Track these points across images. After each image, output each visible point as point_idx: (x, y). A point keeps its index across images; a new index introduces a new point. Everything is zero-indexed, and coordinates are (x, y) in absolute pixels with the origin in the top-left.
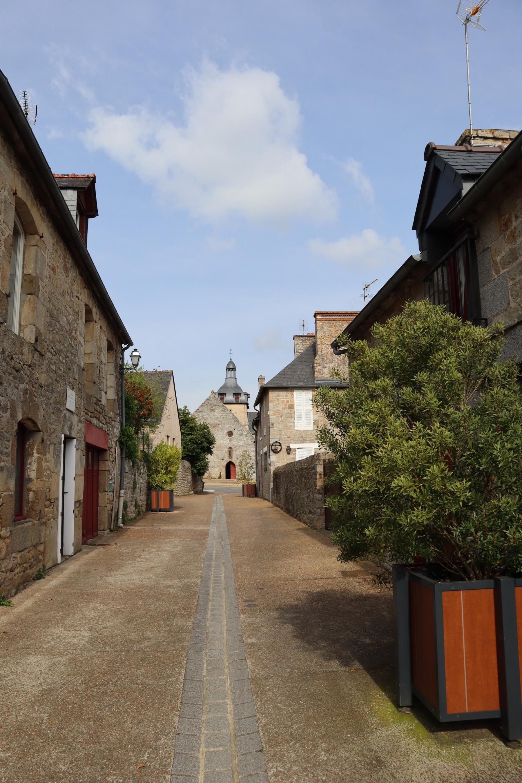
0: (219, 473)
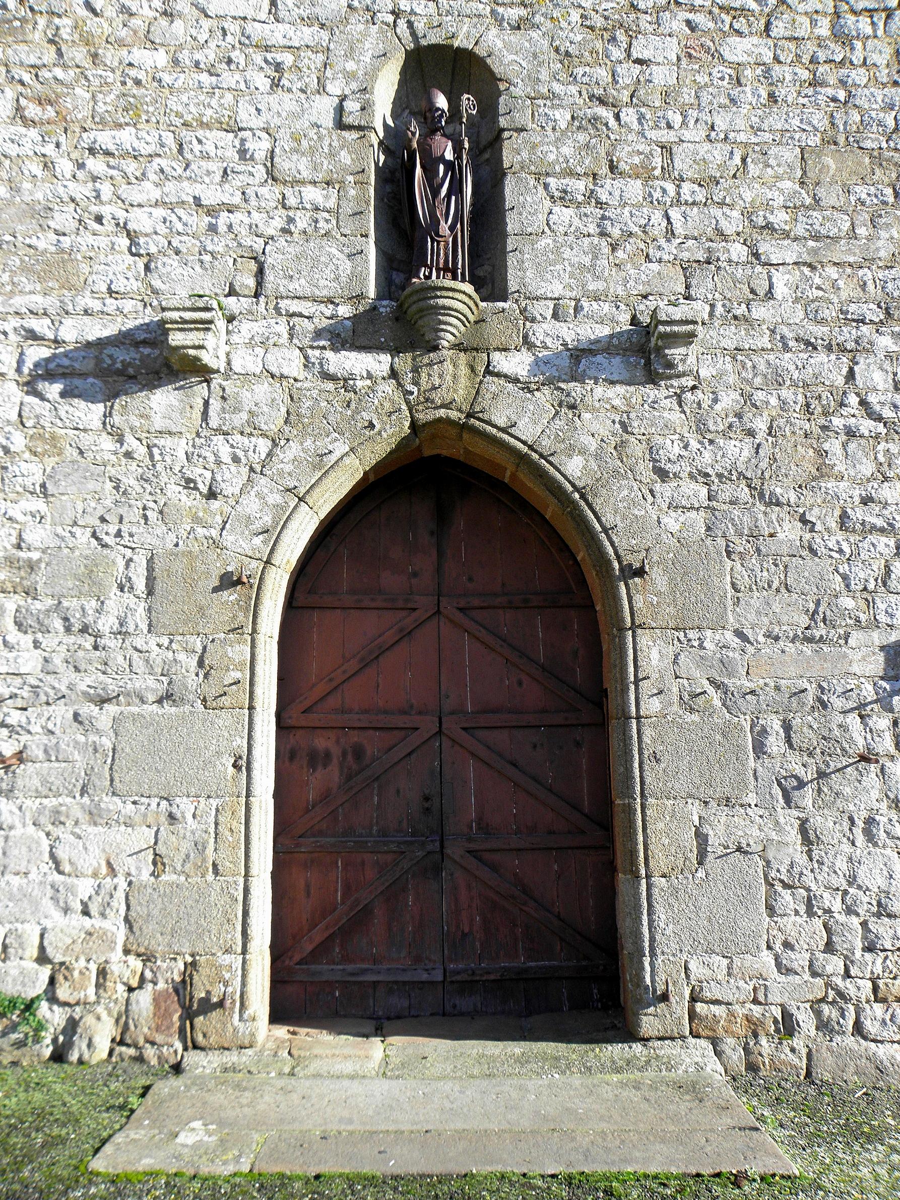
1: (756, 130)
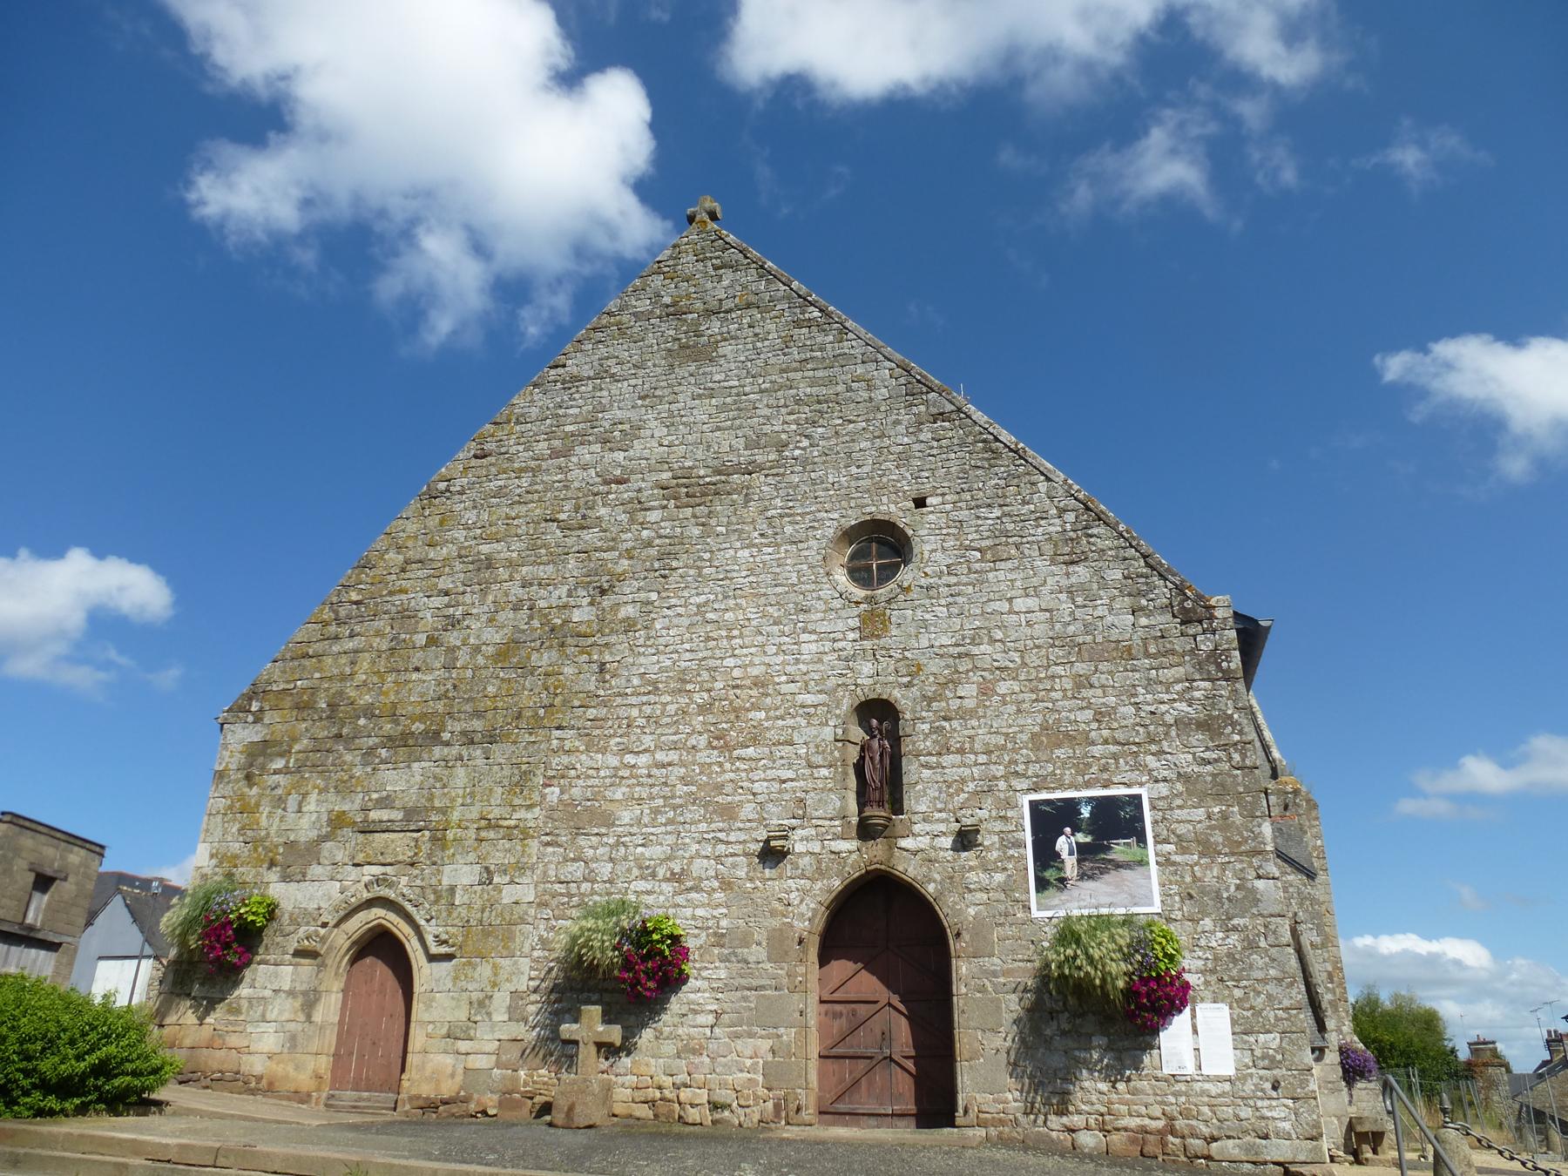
1: (1010, 726)
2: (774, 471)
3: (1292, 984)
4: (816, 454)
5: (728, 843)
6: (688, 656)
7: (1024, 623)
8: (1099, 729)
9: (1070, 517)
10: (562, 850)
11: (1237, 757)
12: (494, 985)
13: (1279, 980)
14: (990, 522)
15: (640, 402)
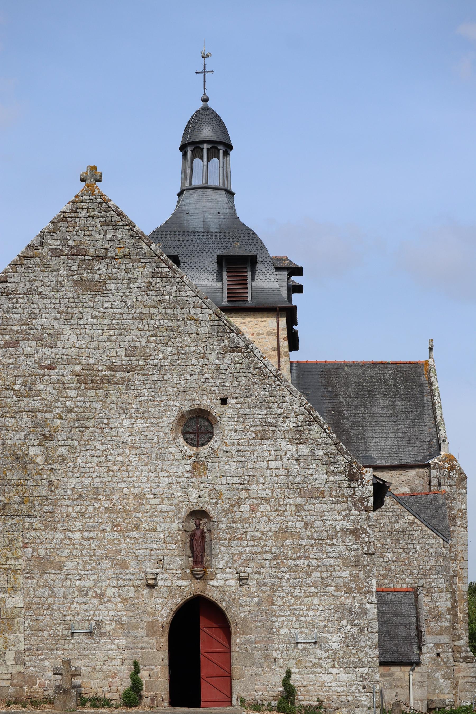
0: (127, 670)
1: (264, 528)
2: (143, 372)
3: (375, 648)
4: (167, 364)
5: (124, 580)
6: (98, 479)
7: (274, 475)
8: (306, 531)
9: (301, 418)
10: (36, 581)
11: (366, 548)
12: (6, 647)
13: (371, 646)
14: (260, 417)
15: (58, 316)
